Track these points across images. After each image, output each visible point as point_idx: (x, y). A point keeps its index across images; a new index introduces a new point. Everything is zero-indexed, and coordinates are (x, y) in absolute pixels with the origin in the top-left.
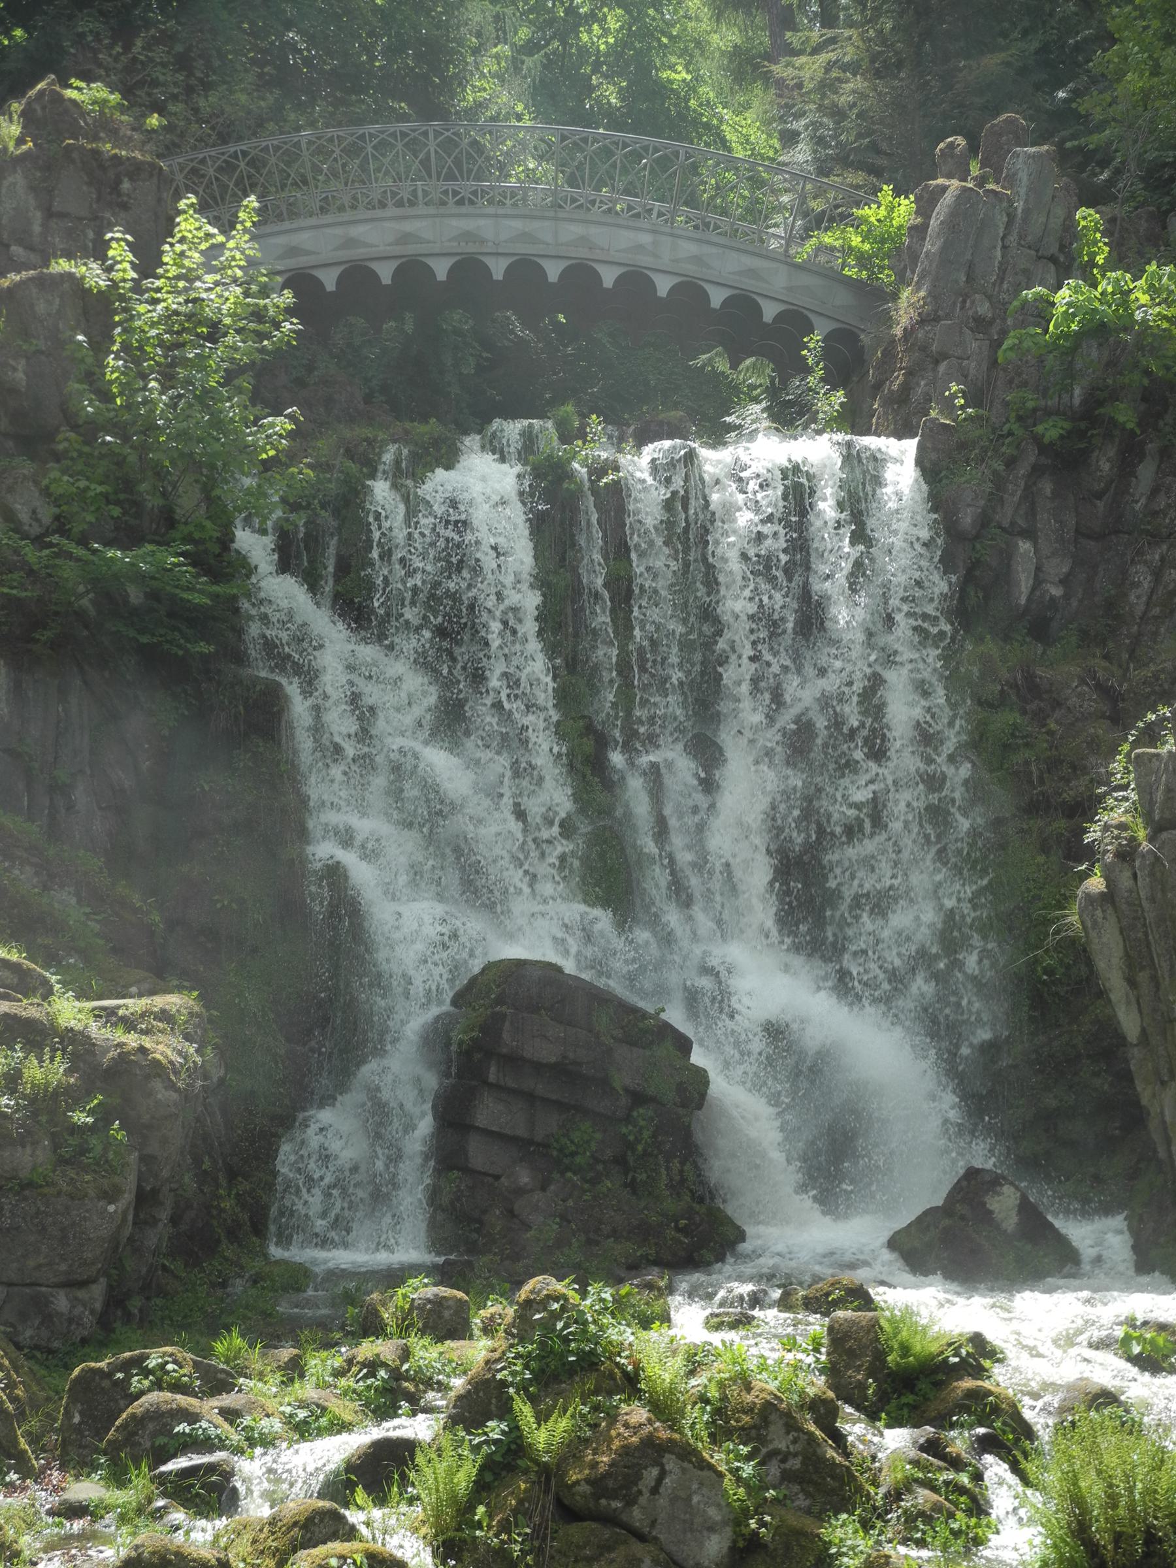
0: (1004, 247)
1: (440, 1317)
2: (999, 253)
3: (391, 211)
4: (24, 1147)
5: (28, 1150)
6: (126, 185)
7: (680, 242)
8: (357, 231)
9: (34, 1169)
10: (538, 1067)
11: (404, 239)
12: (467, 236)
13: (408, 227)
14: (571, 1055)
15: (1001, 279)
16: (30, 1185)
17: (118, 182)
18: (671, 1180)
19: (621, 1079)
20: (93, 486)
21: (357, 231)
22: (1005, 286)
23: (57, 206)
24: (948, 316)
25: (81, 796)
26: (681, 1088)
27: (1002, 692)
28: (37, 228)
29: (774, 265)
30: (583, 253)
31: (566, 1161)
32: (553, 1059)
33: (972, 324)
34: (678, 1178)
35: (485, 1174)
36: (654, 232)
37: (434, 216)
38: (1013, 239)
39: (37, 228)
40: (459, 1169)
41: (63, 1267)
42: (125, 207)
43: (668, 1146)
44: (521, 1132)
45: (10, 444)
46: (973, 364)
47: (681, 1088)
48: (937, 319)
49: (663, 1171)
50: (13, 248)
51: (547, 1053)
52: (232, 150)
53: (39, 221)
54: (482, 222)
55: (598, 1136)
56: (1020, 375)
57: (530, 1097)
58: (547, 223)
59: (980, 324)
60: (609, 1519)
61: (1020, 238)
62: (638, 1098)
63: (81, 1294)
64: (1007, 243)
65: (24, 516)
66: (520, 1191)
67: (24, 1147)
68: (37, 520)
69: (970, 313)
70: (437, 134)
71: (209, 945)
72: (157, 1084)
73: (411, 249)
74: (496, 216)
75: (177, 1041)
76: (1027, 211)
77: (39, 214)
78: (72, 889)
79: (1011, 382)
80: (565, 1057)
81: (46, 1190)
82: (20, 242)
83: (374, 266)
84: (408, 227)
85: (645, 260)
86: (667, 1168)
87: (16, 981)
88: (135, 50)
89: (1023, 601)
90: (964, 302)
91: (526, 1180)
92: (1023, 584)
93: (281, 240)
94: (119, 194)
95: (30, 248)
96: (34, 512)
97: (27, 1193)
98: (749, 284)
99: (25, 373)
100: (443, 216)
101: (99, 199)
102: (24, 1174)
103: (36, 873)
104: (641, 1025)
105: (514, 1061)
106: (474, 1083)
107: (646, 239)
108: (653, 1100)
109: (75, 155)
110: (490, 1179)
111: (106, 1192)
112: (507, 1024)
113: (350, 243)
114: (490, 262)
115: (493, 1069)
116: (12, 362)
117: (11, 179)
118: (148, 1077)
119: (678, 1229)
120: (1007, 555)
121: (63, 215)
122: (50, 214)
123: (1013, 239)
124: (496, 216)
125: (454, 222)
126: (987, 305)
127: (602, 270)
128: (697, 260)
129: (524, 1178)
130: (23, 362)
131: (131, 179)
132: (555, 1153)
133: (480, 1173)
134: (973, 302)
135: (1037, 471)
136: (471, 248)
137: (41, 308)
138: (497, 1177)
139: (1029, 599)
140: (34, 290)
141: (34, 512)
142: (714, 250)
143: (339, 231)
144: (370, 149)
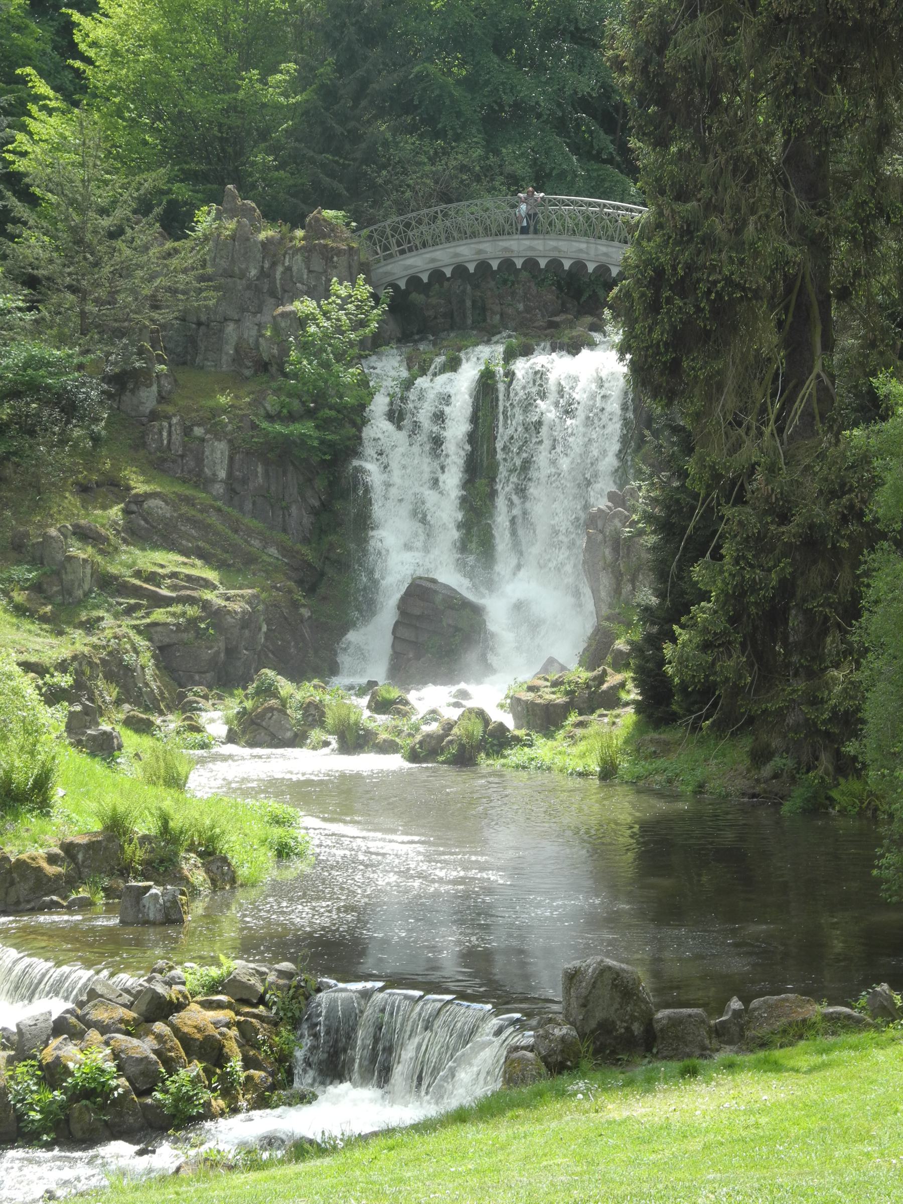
6: (335, 259)
8: (459, 250)
12: (506, 249)
13: (481, 247)
21: (459, 250)
25: (294, 510)
28: (305, 277)
30: (555, 254)
39: (305, 277)
42: (335, 267)
54: (512, 242)
60: (258, 725)
65: (269, 408)
72: (228, 617)
73: (482, 257)
75: (243, 604)
84: (481, 247)
85: (583, 256)
93: (428, 256)
107: (583, 246)
114: (515, 260)
122: (310, 272)
128: (606, 254)
136: (507, 255)
137: (283, 325)
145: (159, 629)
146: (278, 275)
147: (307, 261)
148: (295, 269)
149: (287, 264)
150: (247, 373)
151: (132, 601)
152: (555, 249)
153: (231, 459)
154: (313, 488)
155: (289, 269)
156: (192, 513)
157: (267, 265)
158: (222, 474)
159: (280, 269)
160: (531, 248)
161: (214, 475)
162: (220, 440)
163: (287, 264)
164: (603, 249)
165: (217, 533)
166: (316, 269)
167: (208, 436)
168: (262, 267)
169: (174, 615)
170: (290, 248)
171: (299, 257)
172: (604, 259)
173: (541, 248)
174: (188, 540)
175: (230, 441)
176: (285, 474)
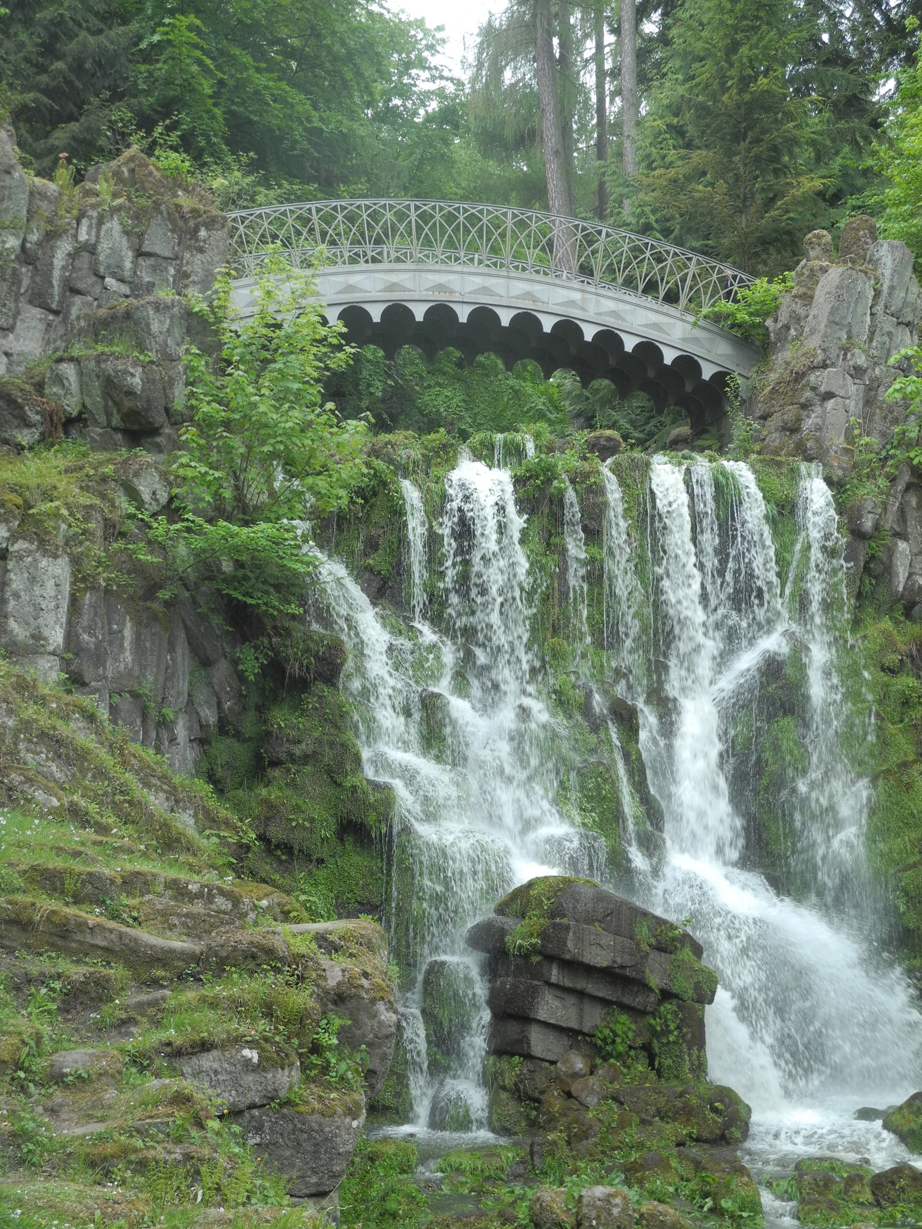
0: (872, 314)
1: (610, 1214)
2: (868, 318)
3: (339, 268)
4: (283, 1069)
5: (286, 1072)
6: (203, 233)
7: (602, 300)
8: (354, 280)
9: (291, 1088)
10: (590, 970)
11: (392, 287)
12: (440, 287)
14: (619, 960)
15: (871, 340)
16: (288, 1103)
17: (196, 230)
18: (693, 1064)
19: (654, 981)
20: (211, 472)
22: (874, 344)
23: (147, 248)
24: (833, 365)
26: (697, 987)
27: (901, 661)
29: (672, 321)
30: (528, 305)
31: (609, 1048)
32: (605, 964)
33: (853, 372)
34: (696, 1063)
35: (543, 1060)
36: (583, 291)
37: (415, 271)
38: (879, 308)
39: (128, 265)
40: (520, 1055)
41: (314, 1180)
42: (201, 250)
43: (689, 1036)
44: (574, 1024)
45: (119, 437)
46: (853, 403)
47: (697, 987)
48: (825, 366)
49: (687, 1058)
50: (107, 279)
51: (599, 958)
52: (234, 216)
53: (130, 259)
54: (452, 277)
55: (633, 1027)
56: (892, 412)
57: (581, 994)
58: (500, 280)
59: (857, 372)
61: (886, 307)
62: (667, 995)
63: (324, 1202)
64: (874, 311)
66: (575, 1075)
67: (283, 1069)
68: (157, 500)
69: (851, 363)
70: (417, 208)
71: (284, 858)
73: (396, 296)
74: (462, 273)
76: (892, 288)
77: (130, 254)
78: (191, 812)
79: (885, 418)
80: (614, 962)
81: (302, 1109)
82: (113, 275)
83: (366, 307)
84: (395, 278)
85: (574, 313)
86: (689, 1055)
87: (230, 906)
88: (156, 134)
89: (901, 589)
90: (845, 354)
91: (580, 1066)
92: (901, 575)
94: (197, 240)
95: (122, 281)
96: (154, 493)
97: (285, 1111)
98: (653, 335)
99: (142, 380)
100: (421, 271)
101: (179, 244)
102: (283, 1094)
103: (167, 798)
104: (670, 934)
105: (574, 966)
106: (536, 982)
107: (576, 296)
108: (676, 996)
109: (163, 208)
110: (547, 1064)
111: (349, 1109)
112: (571, 934)
113: (350, 289)
114: (457, 308)
115: (555, 972)
116: (131, 370)
117: (109, 225)
118: (373, 1001)
119: (715, 1110)
120: (891, 551)
121: (149, 255)
122: (140, 254)
123: (879, 308)
124: (462, 273)
125: (430, 276)
126: (863, 358)
127: (542, 318)
128: (614, 314)
129: (579, 1064)
130: (140, 369)
131: (207, 229)
132: (599, 1042)
133: (539, 1059)
134: (853, 355)
135: (909, 487)
136: (443, 297)
137: (155, 327)
138: (553, 1063)
139: (904, 588)
140: (151, 312)
141: (154, 493)
142: (627, 307)
143: (340, 279)
144: (365, 217)
145: (208, 1061)
146: (59, 259)
147: (135, 237)
148: (104, 247)
149: (83, 237)
150: (25, 437)
151: (77, 972)
152: (529, 295)
153: (74, 601)
154: (210, 684)
155: (91, 249)
156: (44, 721)
157: (34, 237)
158: (56, 637)
159: (64, 247)
160: (485, 290)
161: (37, 637)
162: (56, 557)
163: (83, 237)
164: (610, 305)
165: (101, 774)
166: (157, 249)
167: (20, 545)
168: (24, 240)
169: (237, 1007)
170: (93, 207)
171: (114, 225)
172: (611, 322)
173: (502, 292)
174: (48, 791)
175: (76, 561)
176: (172, 648)
